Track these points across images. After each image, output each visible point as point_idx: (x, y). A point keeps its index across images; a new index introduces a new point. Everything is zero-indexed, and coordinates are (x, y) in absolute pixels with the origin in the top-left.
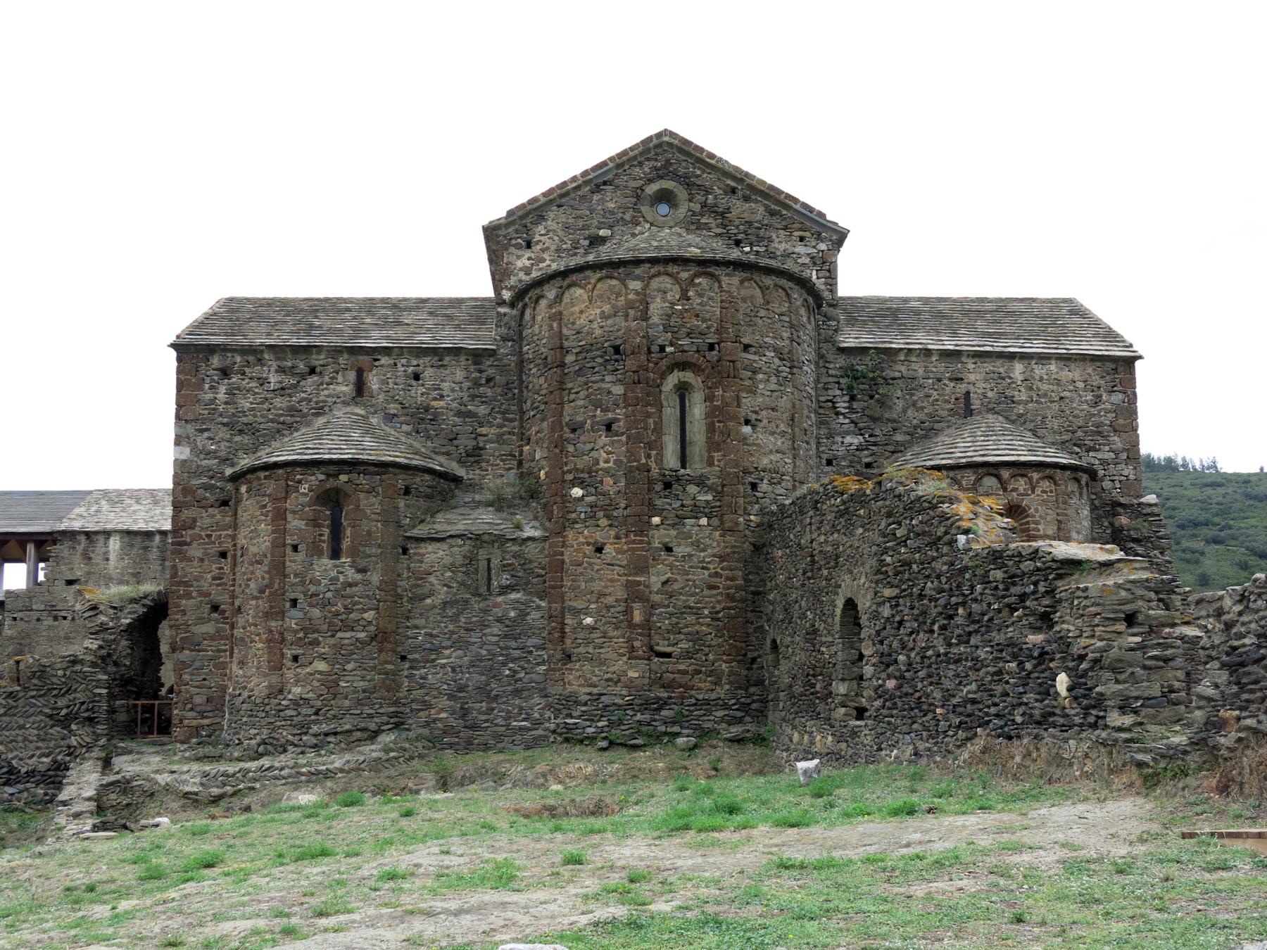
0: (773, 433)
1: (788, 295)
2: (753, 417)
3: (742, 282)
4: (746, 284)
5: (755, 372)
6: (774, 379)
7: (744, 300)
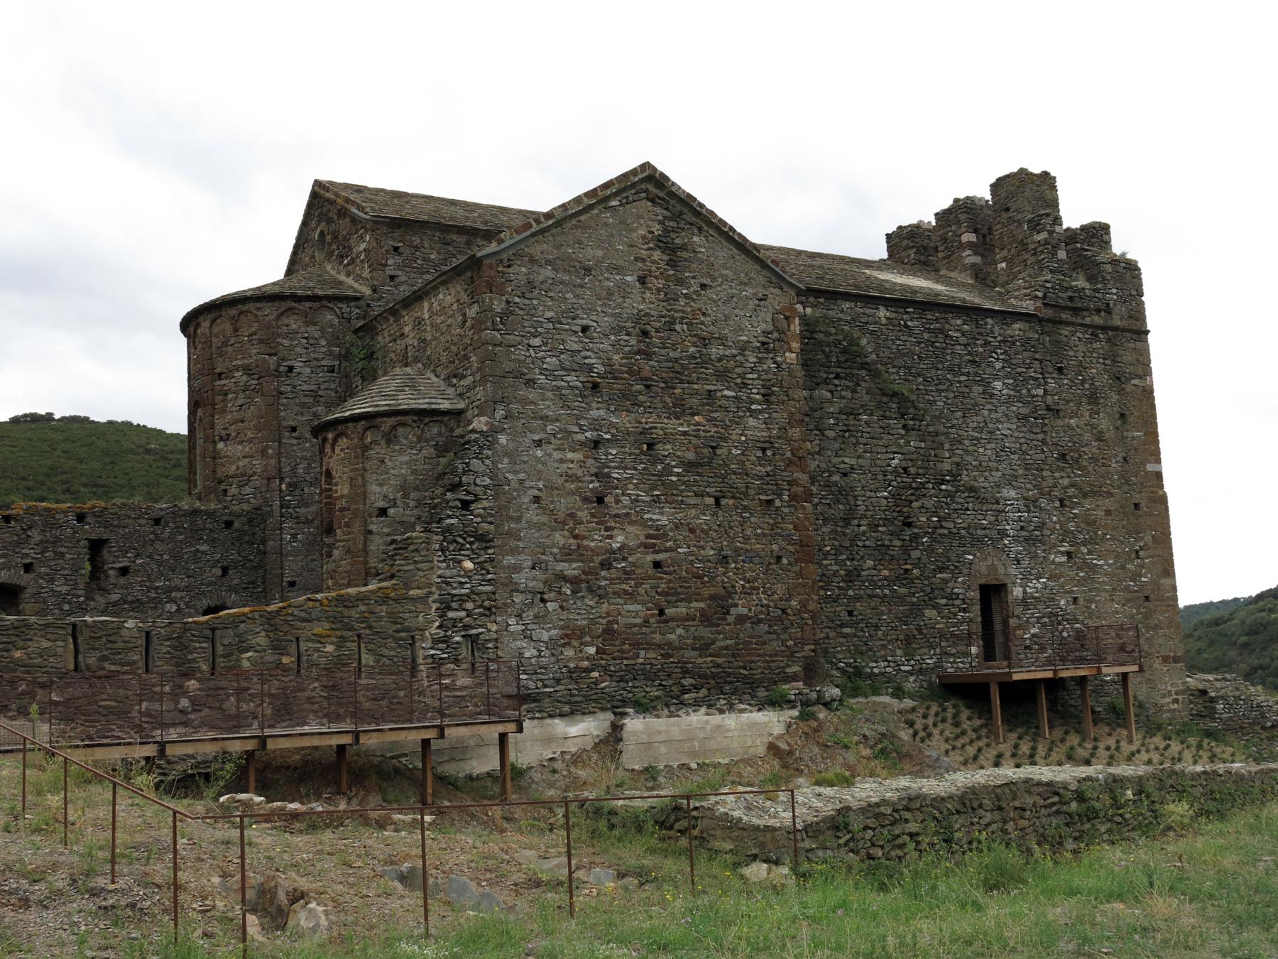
0: (240, 443)
1: (256, 316)
2: (224, 433)
3: (213, 322)
4: (218, 321)
5: (226, 395)
6: (241, 395)
7: (217, 336)
